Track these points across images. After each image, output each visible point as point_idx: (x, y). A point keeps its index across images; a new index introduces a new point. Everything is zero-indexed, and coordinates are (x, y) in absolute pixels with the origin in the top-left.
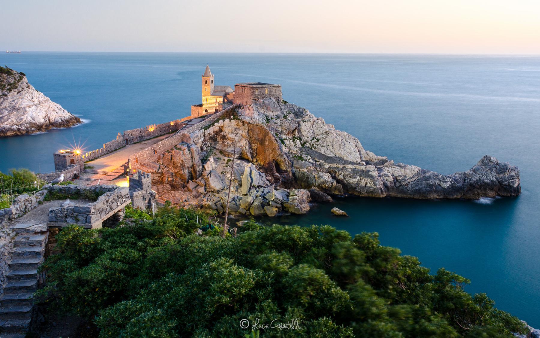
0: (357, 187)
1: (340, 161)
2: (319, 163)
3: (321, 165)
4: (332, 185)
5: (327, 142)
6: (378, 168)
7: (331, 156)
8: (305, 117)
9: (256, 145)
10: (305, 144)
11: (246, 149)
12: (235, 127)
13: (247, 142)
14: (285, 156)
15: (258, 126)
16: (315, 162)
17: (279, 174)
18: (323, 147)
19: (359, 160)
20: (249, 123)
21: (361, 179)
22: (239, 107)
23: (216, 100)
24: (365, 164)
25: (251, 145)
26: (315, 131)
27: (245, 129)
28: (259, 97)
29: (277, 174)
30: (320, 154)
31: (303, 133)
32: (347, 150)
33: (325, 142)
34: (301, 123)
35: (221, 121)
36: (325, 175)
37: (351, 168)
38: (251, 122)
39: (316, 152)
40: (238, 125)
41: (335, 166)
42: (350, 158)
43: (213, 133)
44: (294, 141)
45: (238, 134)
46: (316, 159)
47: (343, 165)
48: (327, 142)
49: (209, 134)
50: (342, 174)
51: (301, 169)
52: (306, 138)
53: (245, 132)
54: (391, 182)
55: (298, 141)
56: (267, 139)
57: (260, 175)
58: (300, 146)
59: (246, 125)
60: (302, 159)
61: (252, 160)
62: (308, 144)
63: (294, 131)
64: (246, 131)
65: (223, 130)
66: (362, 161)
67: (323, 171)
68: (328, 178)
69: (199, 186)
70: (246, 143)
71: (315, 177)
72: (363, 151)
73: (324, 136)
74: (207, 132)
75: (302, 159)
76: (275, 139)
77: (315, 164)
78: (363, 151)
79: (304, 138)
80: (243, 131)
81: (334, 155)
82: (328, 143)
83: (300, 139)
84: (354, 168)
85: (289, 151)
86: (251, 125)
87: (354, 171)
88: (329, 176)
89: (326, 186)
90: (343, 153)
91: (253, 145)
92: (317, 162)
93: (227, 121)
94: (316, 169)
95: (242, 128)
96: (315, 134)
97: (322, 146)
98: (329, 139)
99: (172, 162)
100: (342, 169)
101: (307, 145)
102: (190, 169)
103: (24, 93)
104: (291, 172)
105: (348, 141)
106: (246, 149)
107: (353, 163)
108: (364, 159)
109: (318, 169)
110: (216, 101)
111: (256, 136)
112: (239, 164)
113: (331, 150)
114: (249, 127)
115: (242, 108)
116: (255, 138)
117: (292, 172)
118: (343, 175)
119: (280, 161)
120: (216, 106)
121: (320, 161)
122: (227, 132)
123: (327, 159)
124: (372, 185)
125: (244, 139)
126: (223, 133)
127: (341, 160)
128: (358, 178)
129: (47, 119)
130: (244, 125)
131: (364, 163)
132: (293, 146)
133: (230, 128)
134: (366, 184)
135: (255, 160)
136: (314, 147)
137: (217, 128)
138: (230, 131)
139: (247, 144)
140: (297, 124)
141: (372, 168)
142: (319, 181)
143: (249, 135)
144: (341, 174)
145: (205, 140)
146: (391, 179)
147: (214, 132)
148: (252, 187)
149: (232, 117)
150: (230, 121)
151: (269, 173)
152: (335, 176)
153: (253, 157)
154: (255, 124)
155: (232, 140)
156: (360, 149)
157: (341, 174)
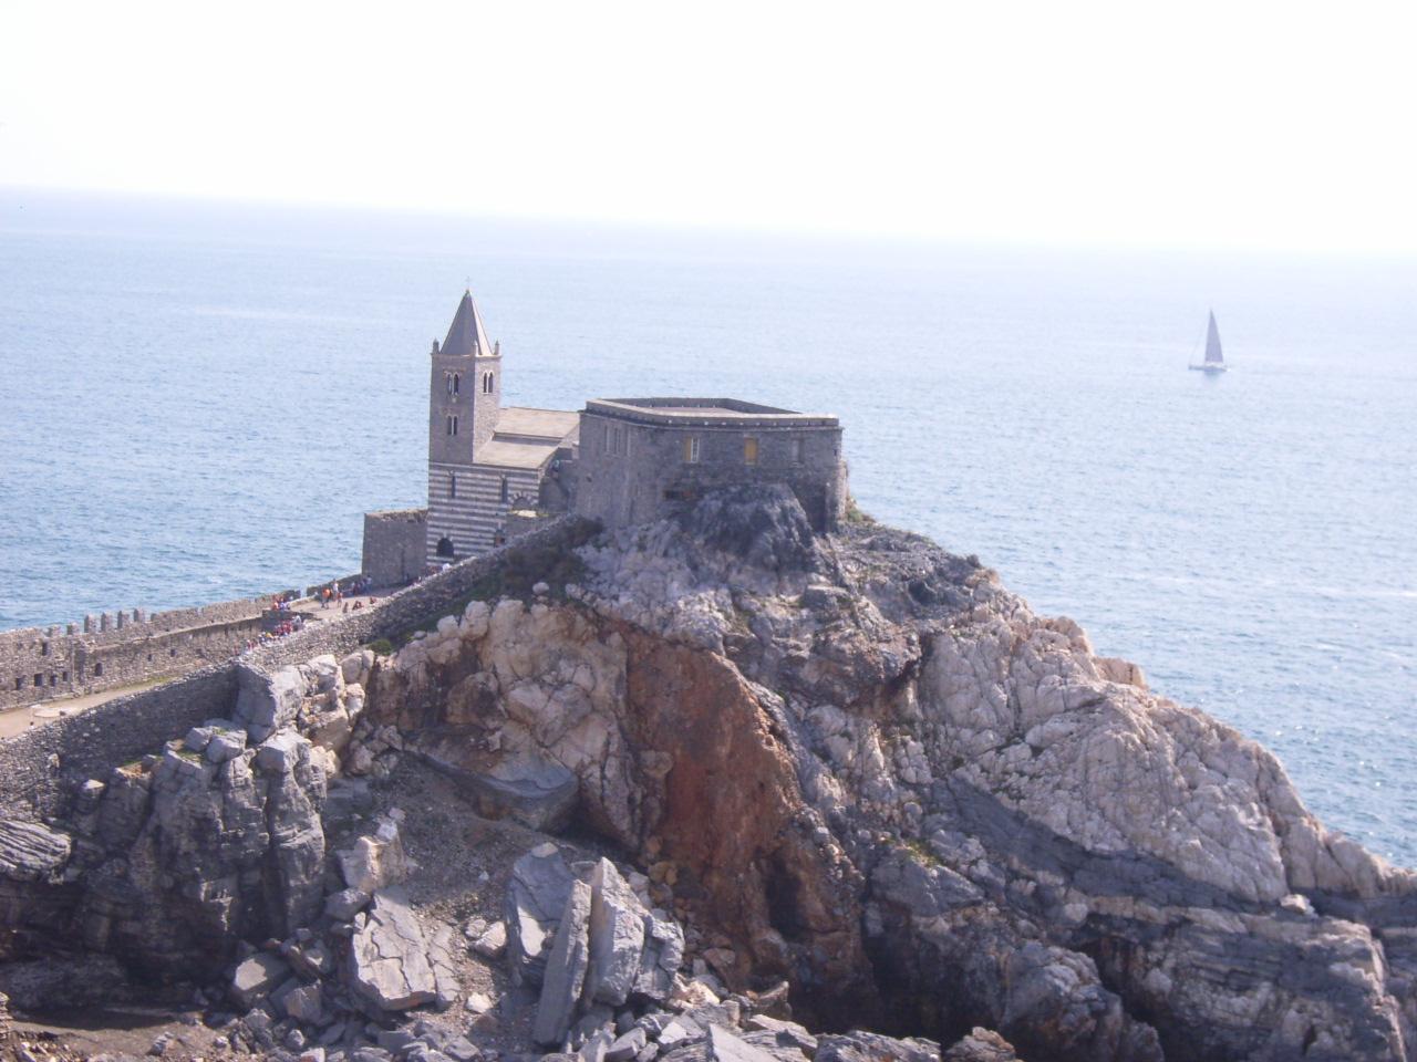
0: (1254, 1047)
1: (1161, 882)
2: (1032, 885)
3: (1042, 904)
4: (1100, 1026)
5: (1087, 762)
6: (1387, 943)
7: (1104, 847)
8: (971, 609)
9: (666, 755)
10: (960, 771)
11: (603, 777)
12: (554, 645)
13: (616, 739)
14: (823, 830)
15: (680, 648)
16: (1009, 881)
17: (786, 936)
18: (1060, 793)
19: (1273, 886)
20: (632, 628)
21: (1279, 1001)
22: (591, 531)
23: (505, 482)
24: (1310, 910)
25: (637, 758)
26: (1027, 693)
27: (606, 661)
28: (706, 482)
29: (774, 938)
30: (1040, 830)
31: (948, 701)
32: (1208, 818)
33: (1072, 760)
35: (476, 608)
36: (1061, 961)
37: (1221, 932)
38: (644, 621)
39: (1019, 818)
40: (569, 632)
41: (1128, 914)
42: (1224, 870)
43: (422, 676)
45: (569, 688)
46: (1016, 863)
47: (1175, 911)
48: (1087, 762)
49: (401, 678)
50: (1169, 964)
51: (916, 919)
52: (967, 734)
53: (605, 676)
55: (915, 746)
56: (727, 727)
57: (648, 935)
58: (927, 777)
59: (616, 639)
61: (635, 841)
62: (976, 768)
63: (896, 684)
64: (615, 671)
65: (486, 662)
66: (1294, 890)
67: (1055, 939)
68: (1075, 979)
69: (293, 980)
70: (608, 744)
71: (999, 973)
73: (1073, 726)
76: (773, 730)
77: (1007, 890)
79: (952, 731)
80: (596, 674)
81: (1121, 846)
82: (1092, 771)
83: (928, 736)
84: (1241, 928)
85: (859, 803)
86: (645, 642)
87: (1234, 944)
88: (1085, 969)
89: (1063, 1027)
90: (1175, 836)
91: (649, 756)
92: (1022, 882)
93: (508, 606)
94: (1013, 925)
95: (591, 651)
96: (1026, 712)
97: (1058, 786)
99: (150, 828)
100: (1170, 929)
101: (972, 774)
102: (254, 877)
104: (856, 931)
105: (1222, 765)
106: (603, 777)
107: (1235, 901)
108: (1309, 883)
109: (1023, 923)
110: (504, 496)
111: (665, 707)
112: (551, 859)
113: (1109, 812)
114: (629, 651)
115: (603, 537)
116: (661, 714)
117: (864, 930)
118: (1175, 972)
119: (798, 862)
120: (500, 522)
121: (1040, 875)
122: (503, 670)
124: (1346, 1047)
125: (597, 718)
126: (480, 677)
128: (1264, 992)
130: (602, 637)
131: (1300, 901)
133: (523, 651)
134: (1311, 1035)
135: (653, 847)
136: (1007, 789)
137: (448, 645)
138: (521, 670)
139: (613, 748)
140: (917, 648)
141: (1356, 933)
142: (1025, 997)
143: (628, 701)
144: (1159, 964)
145: (372, 713)
147: (431, 667)
148: (595, 1001)
149: (541, 586)
150: (527, 610)
151: (727, 925)
152: (1126, 974)
153: (642, 828)
154: (668, 632)
156: (1290, 818)
157: (1159, 964)
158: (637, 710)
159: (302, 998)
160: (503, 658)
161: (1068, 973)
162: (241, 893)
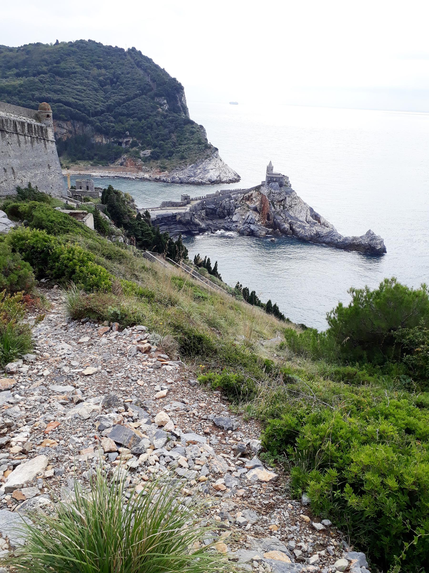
3: (288, 220)
34: (287, 198)
42: (301, 219)
44: (280, 206)
54: (314, 234)
60: (280, 215)
63: (282, 201)
72: (309, 216)
74: (246, 195)
75: (280, 215)
78: (309, 216)
80: (259, 198)
83: (284, 206)
98: (296, 207)
103: (212, 160)
123: (291, 217)
127: (297, 219)
129: (219, 178)
131: (306, 222)
132: (278, 208)
146: (315, 232)
155: (254, 201)
158: (262, 201)
159: (229, 220)
160: (253, 195)
161: (287, 226)
162: (227, 212)
